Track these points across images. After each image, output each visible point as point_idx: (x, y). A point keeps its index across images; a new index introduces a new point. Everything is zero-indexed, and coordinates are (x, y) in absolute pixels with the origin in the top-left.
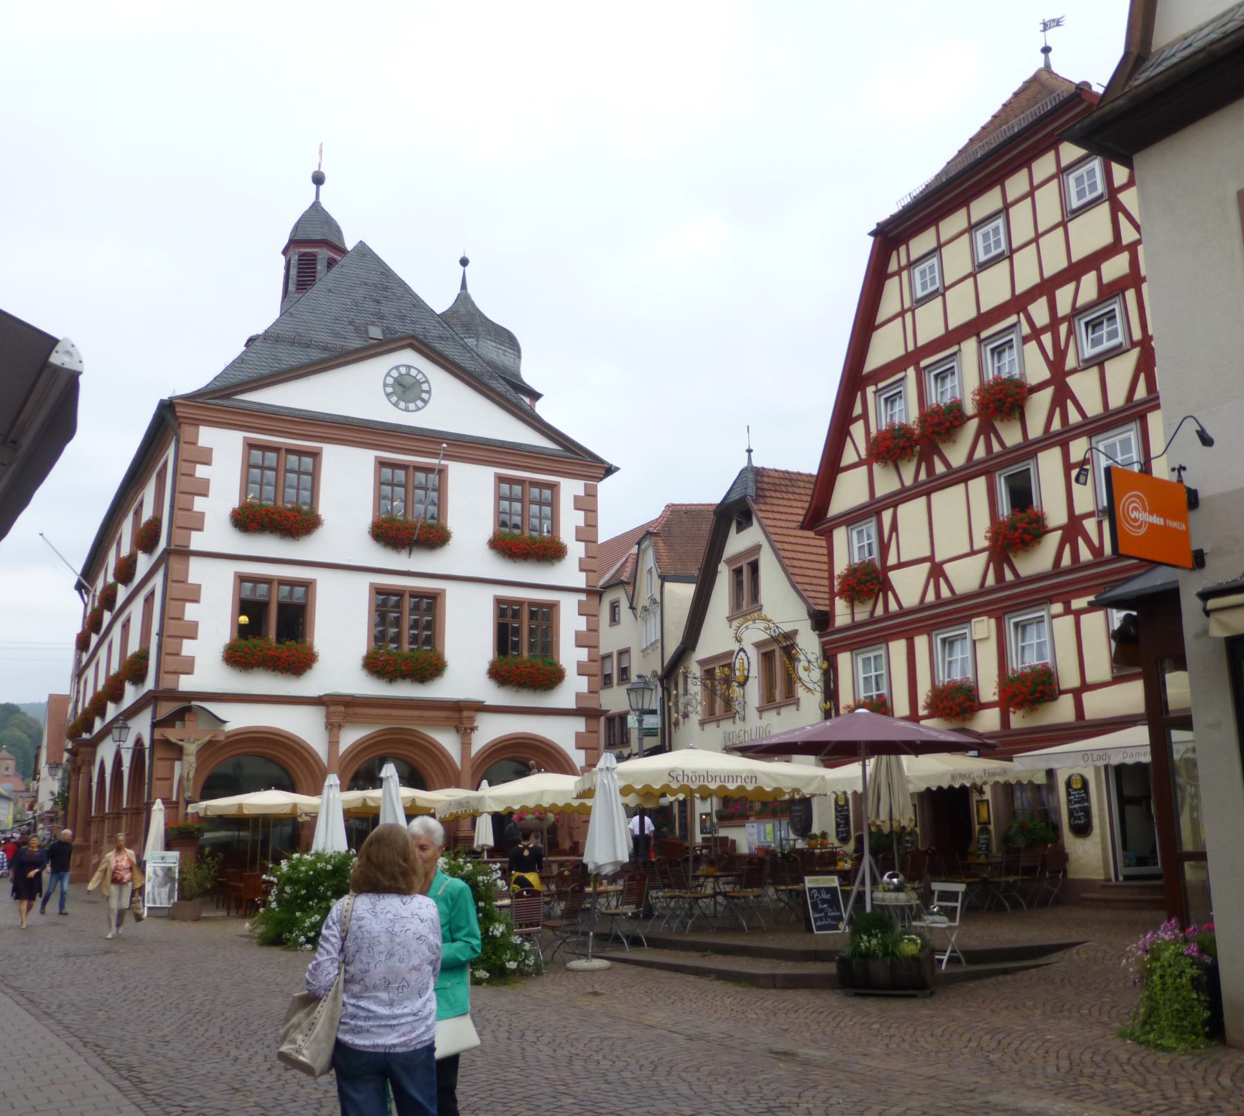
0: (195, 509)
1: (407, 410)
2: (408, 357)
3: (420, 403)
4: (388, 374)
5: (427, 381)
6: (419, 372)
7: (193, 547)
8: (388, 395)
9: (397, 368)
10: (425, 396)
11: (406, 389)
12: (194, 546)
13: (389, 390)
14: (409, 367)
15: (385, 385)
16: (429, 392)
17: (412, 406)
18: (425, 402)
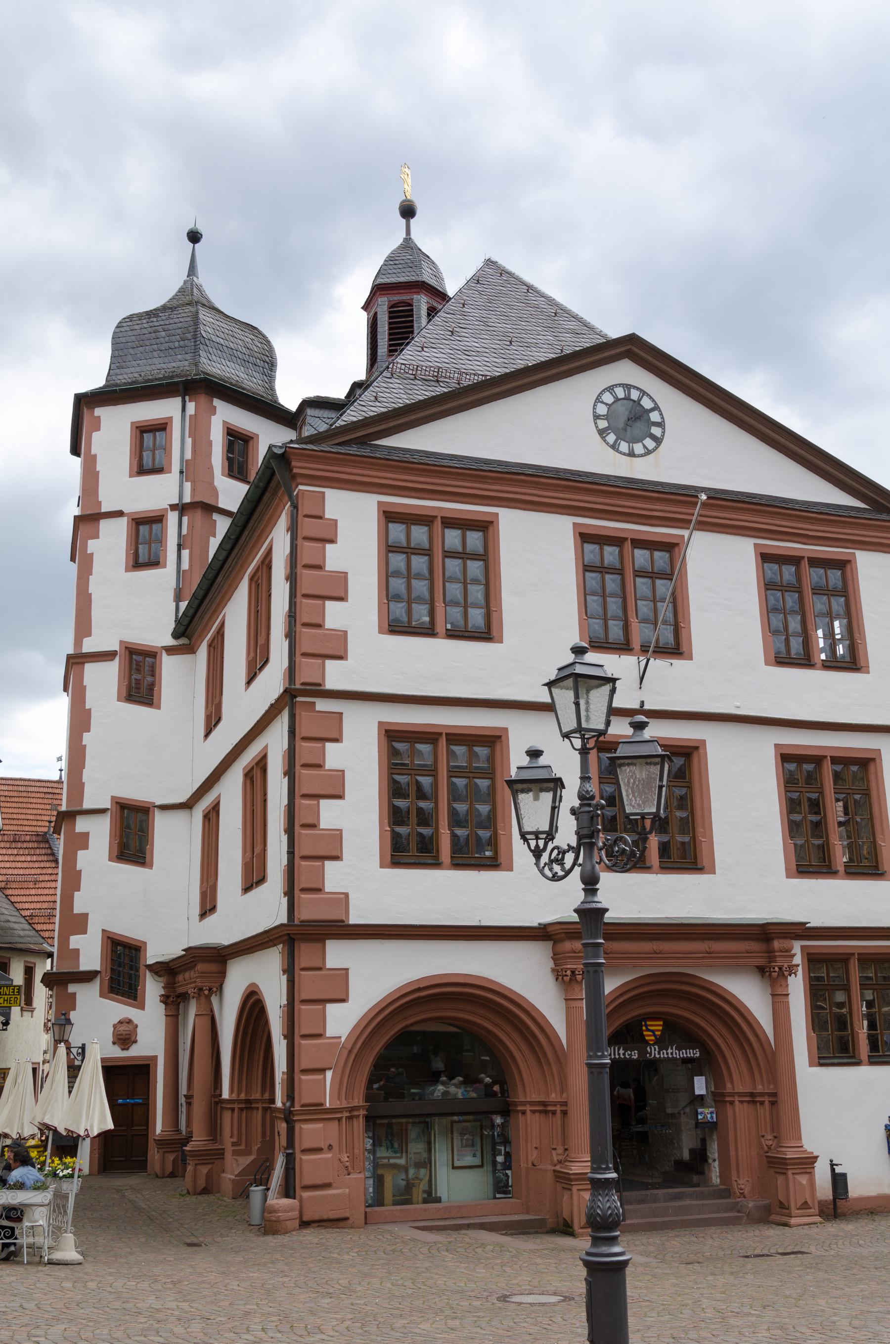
0: (329, 624)
1: (631, 454)
2: (626, 372)
3: (650, 443)
4: (598, 400)
5: (656, 408)
6: (644, 393)
8: (602, 433)
9: (610, 389)
11: (631, 423)
12: (331, 684)
13: (603, 424)
14: (628, 387)
15: (597, 417)
16: (661, 425)
17: (638, 448)
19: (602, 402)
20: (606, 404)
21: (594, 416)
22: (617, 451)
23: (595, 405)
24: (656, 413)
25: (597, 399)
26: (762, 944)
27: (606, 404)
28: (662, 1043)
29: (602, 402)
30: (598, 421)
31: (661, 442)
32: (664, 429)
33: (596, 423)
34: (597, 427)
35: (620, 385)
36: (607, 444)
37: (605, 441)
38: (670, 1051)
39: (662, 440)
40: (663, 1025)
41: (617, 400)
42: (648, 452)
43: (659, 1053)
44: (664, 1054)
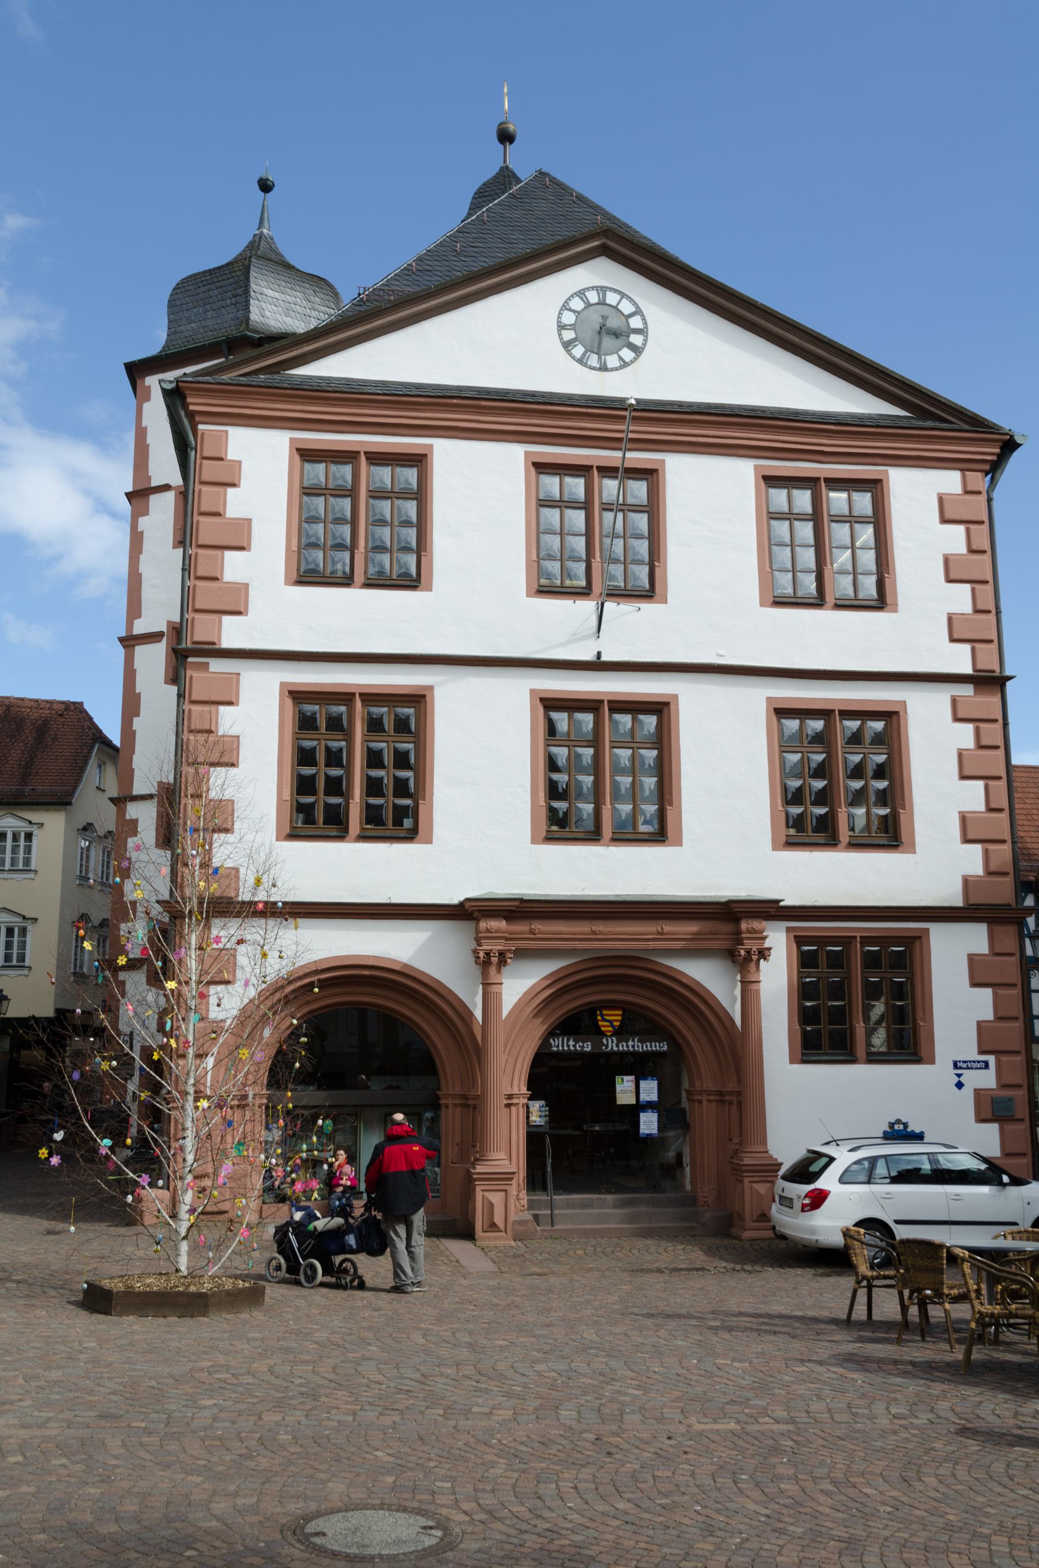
1: (603, 368)
4: (565, 307)
6: (623, 295)
7: (227, 642)
8: (567, 345)
9: (581, 294)
10: (636, 339)
13: (569, 335)
15: (561, 327)
17: (612, 361)
18: (637, 350)
19: (570, 310)
20: (574, 311)
21: (559, 326)
22: (585, 365)
23: (560, 313)
24: (638, 318)
25: (564, 306)
26: (729, 924)
27: (574, 311)
28: (621, 1033)
29: (570, 310)
30: (564, 332)
31: (641, 353)
32: (647, 337)
33: (560, 335)
34: (561, 339)
35: (593, 288)
36: (574, 358)
37: (570, 355)
38: (630, 1043)
39: (643, 349)
40: (623, 1015)
41: (588, 305)
42: (625, 364)
43: (617, 1046)
44: (623, 1047)
